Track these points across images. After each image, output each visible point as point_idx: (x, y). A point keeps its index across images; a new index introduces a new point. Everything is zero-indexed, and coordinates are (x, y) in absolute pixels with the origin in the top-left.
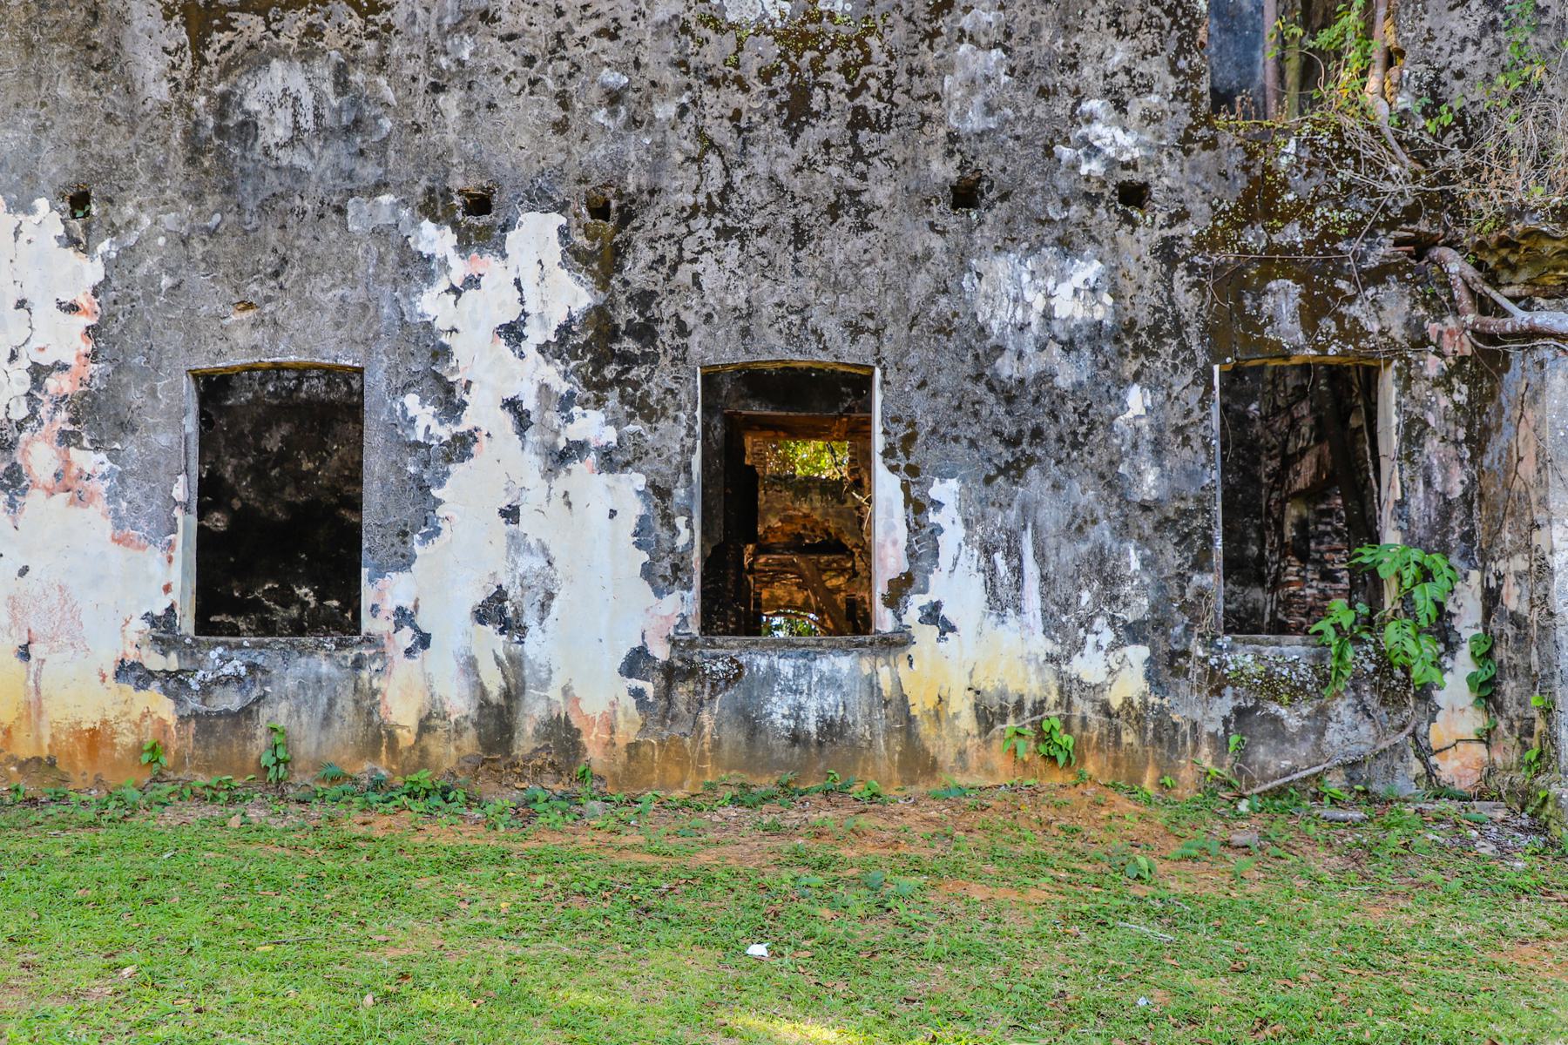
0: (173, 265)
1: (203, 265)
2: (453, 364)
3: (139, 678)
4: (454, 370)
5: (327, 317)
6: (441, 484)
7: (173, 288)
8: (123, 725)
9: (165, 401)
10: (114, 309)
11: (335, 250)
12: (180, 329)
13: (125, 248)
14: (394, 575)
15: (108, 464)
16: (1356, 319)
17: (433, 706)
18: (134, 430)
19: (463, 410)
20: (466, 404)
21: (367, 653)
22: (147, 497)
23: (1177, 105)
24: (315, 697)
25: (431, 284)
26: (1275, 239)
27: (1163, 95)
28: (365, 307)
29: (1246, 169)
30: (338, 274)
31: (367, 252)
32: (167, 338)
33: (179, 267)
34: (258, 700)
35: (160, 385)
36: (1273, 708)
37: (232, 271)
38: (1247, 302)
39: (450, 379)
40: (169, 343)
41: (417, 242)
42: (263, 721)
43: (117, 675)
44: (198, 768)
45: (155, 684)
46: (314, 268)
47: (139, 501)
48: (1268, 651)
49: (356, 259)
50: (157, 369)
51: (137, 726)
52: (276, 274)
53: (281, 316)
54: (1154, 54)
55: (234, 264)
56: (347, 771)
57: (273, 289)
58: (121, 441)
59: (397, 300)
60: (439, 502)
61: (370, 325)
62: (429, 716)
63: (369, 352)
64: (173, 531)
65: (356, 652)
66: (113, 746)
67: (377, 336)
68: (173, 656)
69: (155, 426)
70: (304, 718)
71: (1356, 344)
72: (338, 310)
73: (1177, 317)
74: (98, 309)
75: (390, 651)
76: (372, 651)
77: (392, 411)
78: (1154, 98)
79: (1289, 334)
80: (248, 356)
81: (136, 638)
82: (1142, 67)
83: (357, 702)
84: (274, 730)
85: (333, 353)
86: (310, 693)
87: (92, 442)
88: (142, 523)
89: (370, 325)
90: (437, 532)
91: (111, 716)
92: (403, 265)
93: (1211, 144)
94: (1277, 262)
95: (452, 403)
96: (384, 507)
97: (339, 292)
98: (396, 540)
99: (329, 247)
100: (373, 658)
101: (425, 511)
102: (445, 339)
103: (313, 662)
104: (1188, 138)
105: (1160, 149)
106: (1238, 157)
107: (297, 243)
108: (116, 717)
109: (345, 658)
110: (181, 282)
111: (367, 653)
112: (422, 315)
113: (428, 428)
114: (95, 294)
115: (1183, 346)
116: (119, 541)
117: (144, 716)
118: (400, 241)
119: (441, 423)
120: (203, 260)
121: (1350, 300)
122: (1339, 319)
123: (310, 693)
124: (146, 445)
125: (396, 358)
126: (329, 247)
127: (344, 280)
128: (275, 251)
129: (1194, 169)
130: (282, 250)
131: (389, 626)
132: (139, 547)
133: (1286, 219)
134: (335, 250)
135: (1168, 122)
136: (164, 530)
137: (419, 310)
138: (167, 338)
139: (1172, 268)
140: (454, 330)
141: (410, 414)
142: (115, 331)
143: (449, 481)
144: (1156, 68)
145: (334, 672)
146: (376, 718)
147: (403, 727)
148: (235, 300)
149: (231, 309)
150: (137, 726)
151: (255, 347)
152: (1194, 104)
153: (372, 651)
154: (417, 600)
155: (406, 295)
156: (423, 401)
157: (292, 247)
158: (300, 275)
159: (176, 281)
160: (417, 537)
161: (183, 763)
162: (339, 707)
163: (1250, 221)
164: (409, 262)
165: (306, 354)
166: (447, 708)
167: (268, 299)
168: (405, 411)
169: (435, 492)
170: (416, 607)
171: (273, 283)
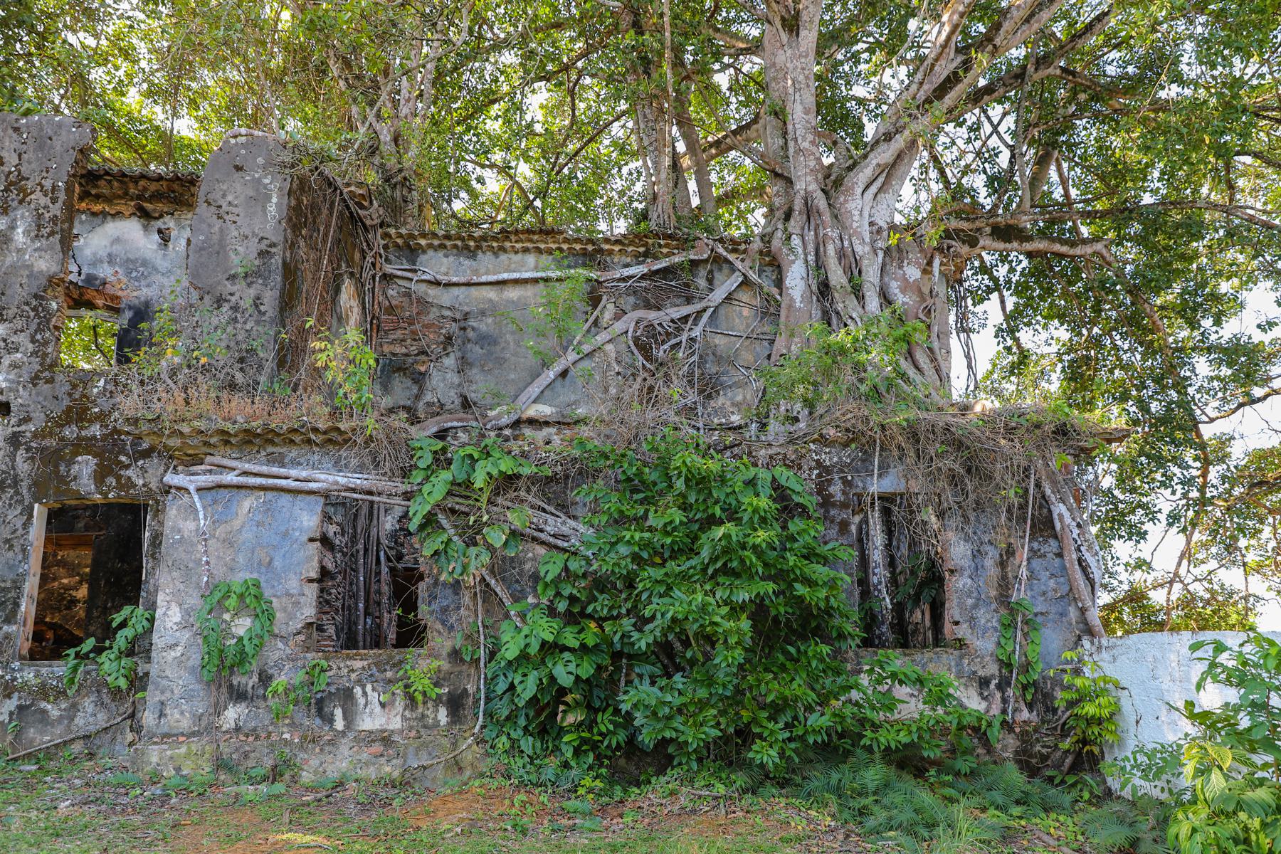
16: (129, 478)
23: (32, 359)
26: (83, 433)
27: (24, 353)
29: (70, 395)
36: (43, 704)
38: (62, 468)
48: (44, 671)
54: (22, 331)
71: (127, 492)
73: (16, 476)
78: (19, 355)
79: (86, 485)
82: (14, 338)
93: (50, 381)
94: (84, 446)
104: (37, 377)
105: (19, 383)
106: (67, 387)
115: (17, 493)
121: (127, 467)
122: (119, 478)
129: (38, 394)
133: (91, 421)
135: (25, 369)
139: (16, 449)
144: (22, 339)
152: (43, 359)
163: (69, 423)
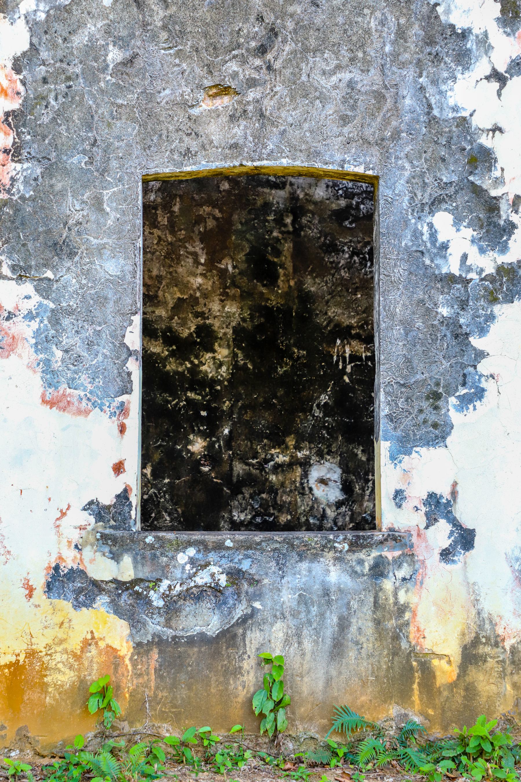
0: (124, 33)
1: (164, 35)
2: (497, 173)
3: (78, 592)
4: (499, 182)
5: (330, 109)
6: (483, 331)
7: (124, 64)
8: (58, 657)
9: (113, 215)
10: (42, 89)
11: (340, 20)
12: (134, 120)
13: (58, 8)
14: (423, 450)
15: (36, 299)
17: (481, 627)
18: (72, 254)
19: (510, 233)
20: (513, 226)
21: (390, 555)
22: (90, 344)
24: (322, 615)
25: (466, 68)
28: (380, 97)
30: (344, 51)
31: (382, 23)
32: (116, 131)
33: (132, 36)
34: (244, 620)
35: (107, 194)
37: (203, 43)
39: (494, 193)
40: (119, 138)
41: (448, 12)
42: (251, 649)
43: (49, 587)
44: (163, 717)
45: (103, 600)
46: (312, 43)
47: (80, 350)
49: (368, 32)
50: (103, 172)
51: (78, 658)
52: (262, 50)
53: (268, 105)
55: (206, 35)
56: (368, 717)
57: (258, 69)
58: (54, 268)
59: (422, 88)
60: (481, 355)
61: (386, 122)
62: (476, 642)
63: (386, 156)
64: (126, 390)
65: (375, 553)
66: (44, 687)
67: (396, 135)
68: (127, 560)
69: (101, 248)
70: (308, 645)
72: (345, 100)
74: (21, 88)
75: (421, 553)
76: (397, 553)
77: (417, 234)
80: (225, 158)
81: (75, 536)
83: (378, 622)
84: (268, 661)
85: (338, 157)
86: (314, 610)
87: (13, 268)
88: (84, 379)
89: (386, 122)
90: (480, 394)
91: (40, 645)
92: (430, 41)
95: (496, 225)
96: (408, 361)
97: (346, 76)
98: (425, 404)
99: (332, 16)
100: (398, 563)
101: (463, 366)
102: (485, 141)
103: (317, 568)
107: (291, 9)
108: (48, 646)
109: (361, 562)
110: (135, 56)
111: (390, 555)
112: (455, 109)
113: (465, 257)
114: (17, 68)
116: (52, 403)
117: (86, 644)
118: (425, 10)
119: (482, 251)
120: (164, 27)
123: (314, 610)
124: (87, 273)
125: (422, 164)
126: (332, 16)
127: (352, 60)
128: (260, 18)
130: (269, 18)
131: (420, 519)
132: (79, 412)
134: (340, 20)
136: (113, 389)
137: (451, 102)
138: (116, 131)
140: (497, 129)
141: (441, 238)
142: (46, 119)
143: (494, 328)
145: (347, 581)
146: (404, 645)
147: (440, 657)
148: (207, 83)
149: (201, 95)
150: (78, 658)
151: (235, 146)
153: (397, 553)
154: (455, 484)
155: (435, 82)
156: (457, 222)
157: (283, 15)
158: (294, 52)
159: (128, 54)
160: (453, 400)
161: (142, 709)
162: (353, 629)
164: (439, 38)
165: (302, 156)
166: (500, 631)
167: (252, 83)
168: (433, 235)
169: (475, 341)
170: (454, 494)
171: (258, 62)
